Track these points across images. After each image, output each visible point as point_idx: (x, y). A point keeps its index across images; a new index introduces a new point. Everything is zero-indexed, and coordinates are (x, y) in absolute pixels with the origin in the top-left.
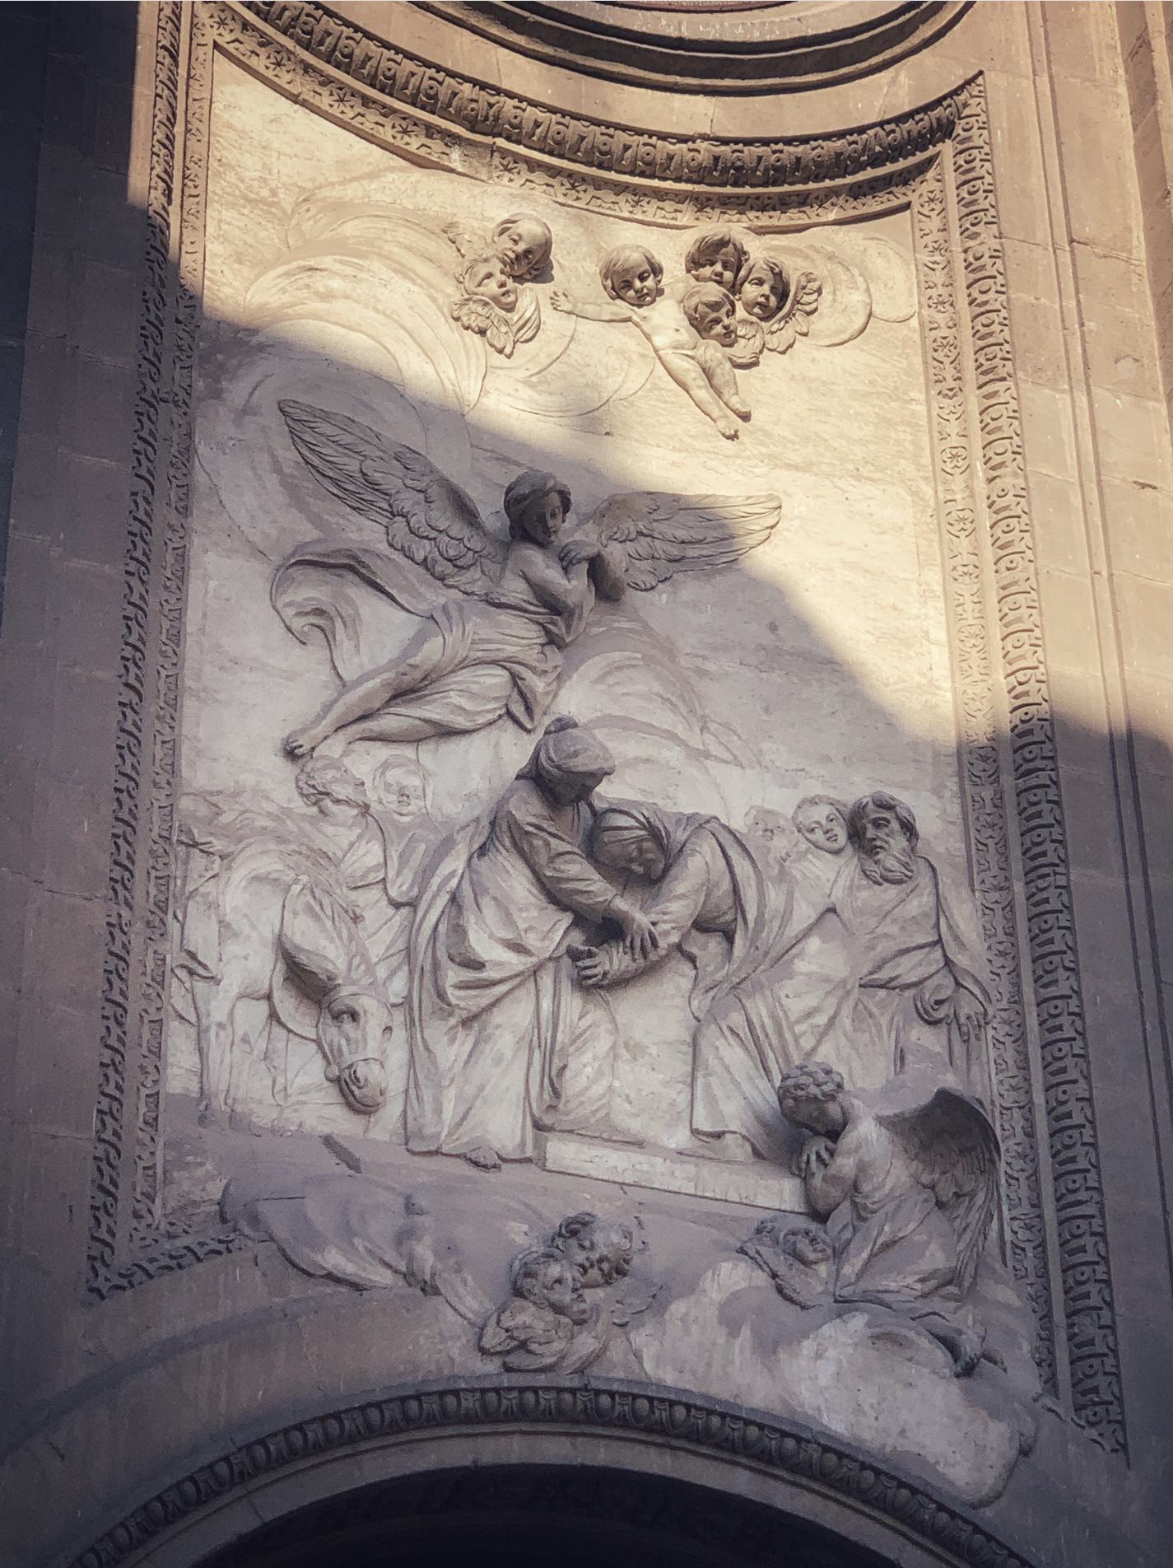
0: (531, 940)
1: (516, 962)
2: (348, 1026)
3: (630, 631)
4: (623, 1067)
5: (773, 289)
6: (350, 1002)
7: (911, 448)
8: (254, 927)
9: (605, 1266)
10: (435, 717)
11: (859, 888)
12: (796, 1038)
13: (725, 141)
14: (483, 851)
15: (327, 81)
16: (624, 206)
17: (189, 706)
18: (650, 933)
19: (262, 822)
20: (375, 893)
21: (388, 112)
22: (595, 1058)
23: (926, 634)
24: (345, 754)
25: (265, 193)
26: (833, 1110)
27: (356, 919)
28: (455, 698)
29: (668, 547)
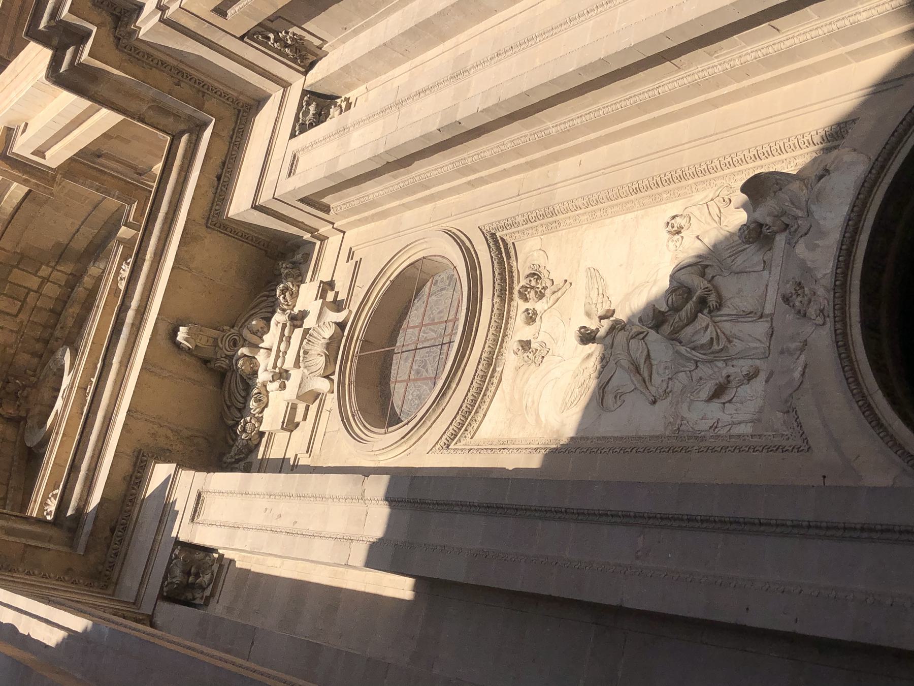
0: (704, 325)
2: (731, 378)
6: (723, 378)
10: (643, 360)
13: (494, 294)
14: (680, 342)
15: (479, 406)
16: (511, 321)
17: (641, 434)
18: (704, 289)
19: (673, 410)
23: (623, 221)
25: (508, 422)
26: (752, 226)
27: (701, 379)
28: (638, 355)
29: (599, 298)
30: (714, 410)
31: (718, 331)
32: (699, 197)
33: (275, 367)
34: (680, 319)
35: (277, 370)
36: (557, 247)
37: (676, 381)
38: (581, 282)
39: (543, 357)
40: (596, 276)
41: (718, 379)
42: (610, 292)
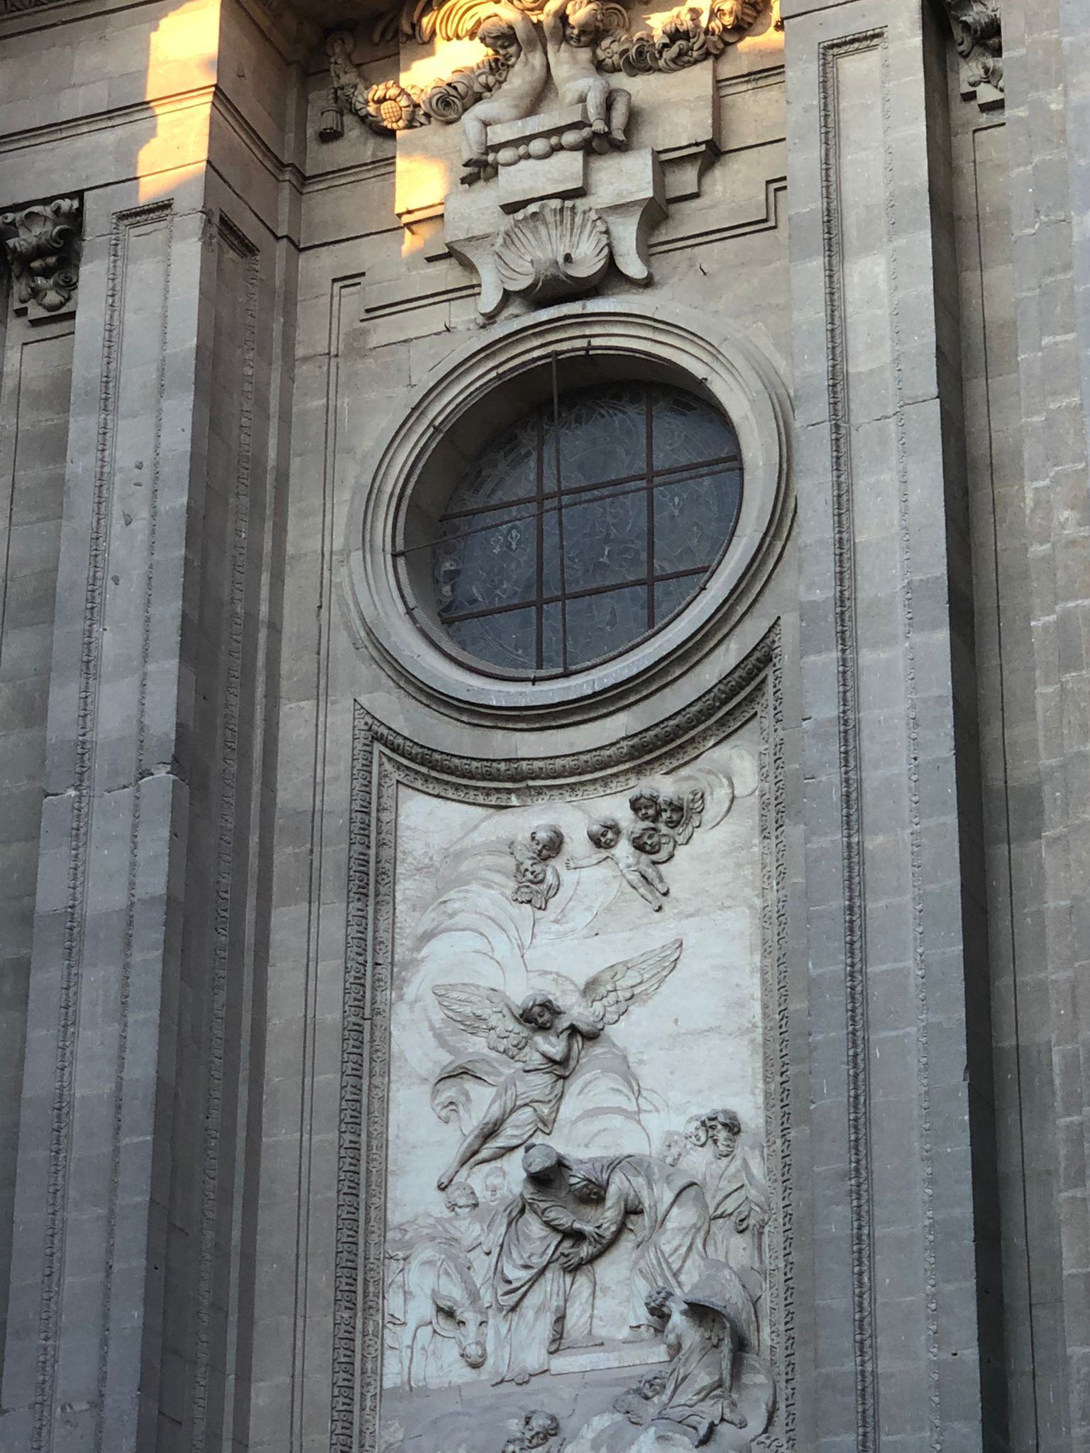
0: (535, 1260)
1: (526, 1275)
2: (463, 1328)
3: (602, 1054)
4: (598, 1302)
5: (672, 810)
8: (421, 1288)
9: (541, 1435)
10: (501, 1145)
11: (711, 1163)
14: (522, 1211)
19: (425, 1231)
20: (478, 1250)
21: (477, 788)
22: (581, 1304)
24: (469, 1176)
25: (427, 861)
26: (665, 1309)
30: (422, 1308)
31: (524, 1289)
32: (757, 1168)
33: (496, 148)
34: (545, 1209)
35: (491, 158)
36: (733, 843)
37: (469, 1220)
38: (660, 933)
39: (529, 902)
40: (665, 968)
41: (463, 1306)
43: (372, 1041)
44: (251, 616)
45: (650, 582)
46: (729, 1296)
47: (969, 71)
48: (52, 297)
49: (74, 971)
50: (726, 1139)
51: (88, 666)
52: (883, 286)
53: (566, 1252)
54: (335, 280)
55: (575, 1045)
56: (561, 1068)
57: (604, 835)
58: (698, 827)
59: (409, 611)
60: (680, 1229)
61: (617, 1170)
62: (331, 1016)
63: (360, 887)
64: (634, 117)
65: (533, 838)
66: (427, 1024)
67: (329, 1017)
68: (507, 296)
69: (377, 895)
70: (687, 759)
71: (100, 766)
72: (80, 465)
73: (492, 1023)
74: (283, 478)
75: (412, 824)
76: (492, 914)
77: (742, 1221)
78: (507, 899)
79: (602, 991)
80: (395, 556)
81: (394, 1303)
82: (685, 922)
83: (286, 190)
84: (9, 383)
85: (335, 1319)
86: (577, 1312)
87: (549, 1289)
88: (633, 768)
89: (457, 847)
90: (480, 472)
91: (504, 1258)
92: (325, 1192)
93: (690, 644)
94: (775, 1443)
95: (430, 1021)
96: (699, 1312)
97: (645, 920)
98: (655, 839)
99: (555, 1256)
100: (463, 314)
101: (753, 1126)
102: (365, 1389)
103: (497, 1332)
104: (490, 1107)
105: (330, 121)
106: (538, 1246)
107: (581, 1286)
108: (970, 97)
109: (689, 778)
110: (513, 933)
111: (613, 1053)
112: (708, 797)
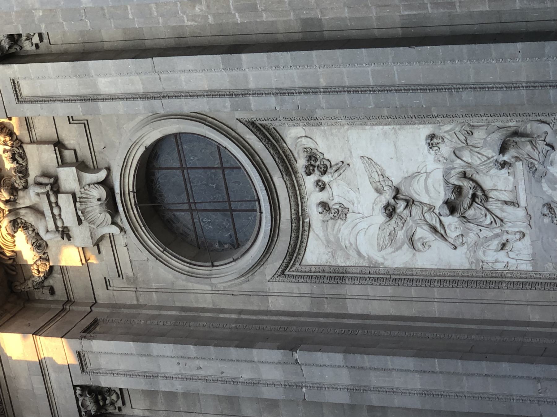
0: (483, 212)
1: (489, 216)
2: (509, 240)
3: (404, 187)
4: (499, 188)
5: (311, 160)
7: (337, 130)
9: (550, 210)
11: (446, 145)
12: (485, 161)
14: (464, 217)
19: (472, 254)
21: (302, 235)
24: (451, 238)
25: (330, 254)
26: (502, 163)
32: (448, 127)
33: (57, 227)
35: (60, 229)
36: (323, 136)
38: (358, 165)
39: (346, 215)
40: (371, 163)
41: (501, 240)
42: (388, 174)
43: (399, 275)
44: (236, 321)
45: (223, 169)
46: (497, 138)
47: (27, 46)
48: (114, 397)
49: (372, 389)
50: (437, 139)
51: (255, 383)
52: (110, 79)
53: (480, 200)
54: (107, 289)
55: (401, 197)
56: (410, 203)
57: (320, 186)
58: (317, 150)
59: (234, 260)
60: (471, 157)
61: (449, 181)
62: (390, 290)
63: (340, 280)
64: (45, 175)
65: (321, 213)
66: (393, 254)
67: (390, 291)
68: (114, 223)
69: (343, 273)
70: (291, 154)
71: (294, 379)
72: (178, 387)
73: (392, 229)
74: (183, 309)
75: (316, 259)
76: (351, 229)
77: (468, 133)
78: (345, 223)
79: (380, 187)
80: (213, 266)
81: (500, 266)
82: (353, 155)
83: (73, 308)
84: (147, 413)
85: (506, 289)
86: (503, 196)
87: (494, 207)
88: (294, 175)
89: (325, 242)
90: (181, 234)
91: (482, 224)
92: (457, 293)
93: (247, 153)
94: (553, 120)
95: (391, 253)
96: (503, 150)
97: (353, 170)
98: (322, 166)
99: (482, 205)
100: (120, 240)
101: (432, 129)
102: (533, 277)
103: (511, 227)
104: (424, 230)
105: (46, 291)
106: (478, 211)
107: (493, 195)
108: (37, 46)
109: (298, 153)
110: (357, 221)
111: (404, 183)
112: (306, 146)
